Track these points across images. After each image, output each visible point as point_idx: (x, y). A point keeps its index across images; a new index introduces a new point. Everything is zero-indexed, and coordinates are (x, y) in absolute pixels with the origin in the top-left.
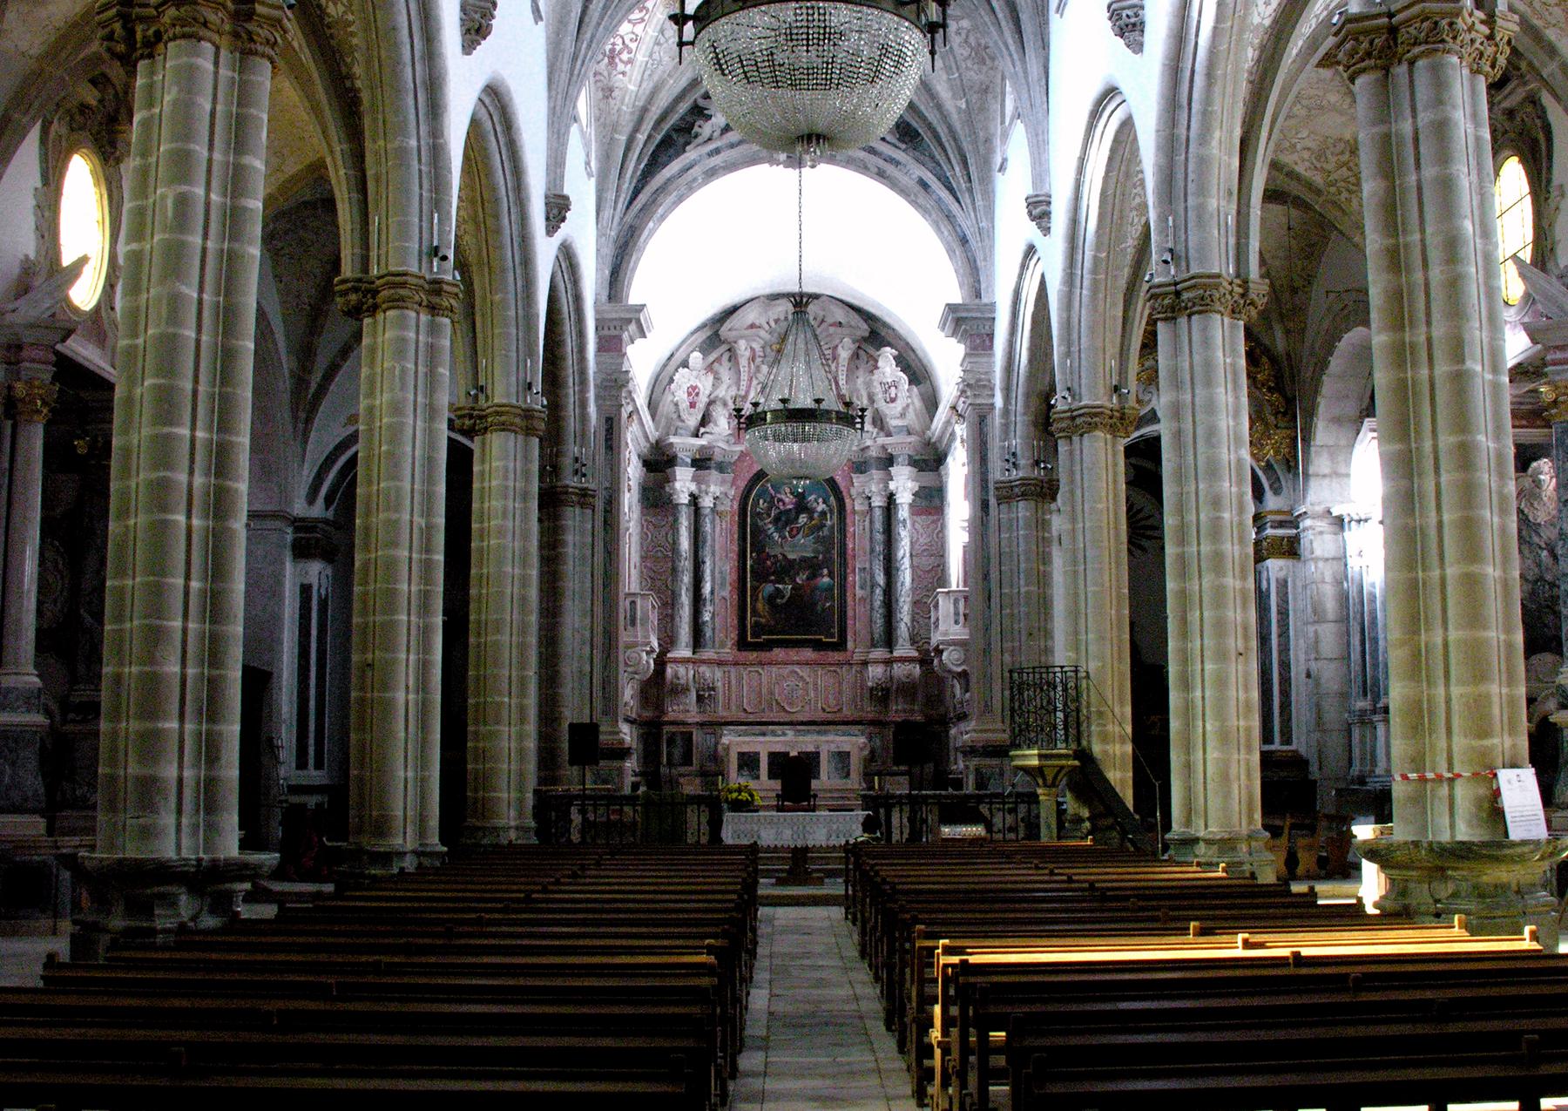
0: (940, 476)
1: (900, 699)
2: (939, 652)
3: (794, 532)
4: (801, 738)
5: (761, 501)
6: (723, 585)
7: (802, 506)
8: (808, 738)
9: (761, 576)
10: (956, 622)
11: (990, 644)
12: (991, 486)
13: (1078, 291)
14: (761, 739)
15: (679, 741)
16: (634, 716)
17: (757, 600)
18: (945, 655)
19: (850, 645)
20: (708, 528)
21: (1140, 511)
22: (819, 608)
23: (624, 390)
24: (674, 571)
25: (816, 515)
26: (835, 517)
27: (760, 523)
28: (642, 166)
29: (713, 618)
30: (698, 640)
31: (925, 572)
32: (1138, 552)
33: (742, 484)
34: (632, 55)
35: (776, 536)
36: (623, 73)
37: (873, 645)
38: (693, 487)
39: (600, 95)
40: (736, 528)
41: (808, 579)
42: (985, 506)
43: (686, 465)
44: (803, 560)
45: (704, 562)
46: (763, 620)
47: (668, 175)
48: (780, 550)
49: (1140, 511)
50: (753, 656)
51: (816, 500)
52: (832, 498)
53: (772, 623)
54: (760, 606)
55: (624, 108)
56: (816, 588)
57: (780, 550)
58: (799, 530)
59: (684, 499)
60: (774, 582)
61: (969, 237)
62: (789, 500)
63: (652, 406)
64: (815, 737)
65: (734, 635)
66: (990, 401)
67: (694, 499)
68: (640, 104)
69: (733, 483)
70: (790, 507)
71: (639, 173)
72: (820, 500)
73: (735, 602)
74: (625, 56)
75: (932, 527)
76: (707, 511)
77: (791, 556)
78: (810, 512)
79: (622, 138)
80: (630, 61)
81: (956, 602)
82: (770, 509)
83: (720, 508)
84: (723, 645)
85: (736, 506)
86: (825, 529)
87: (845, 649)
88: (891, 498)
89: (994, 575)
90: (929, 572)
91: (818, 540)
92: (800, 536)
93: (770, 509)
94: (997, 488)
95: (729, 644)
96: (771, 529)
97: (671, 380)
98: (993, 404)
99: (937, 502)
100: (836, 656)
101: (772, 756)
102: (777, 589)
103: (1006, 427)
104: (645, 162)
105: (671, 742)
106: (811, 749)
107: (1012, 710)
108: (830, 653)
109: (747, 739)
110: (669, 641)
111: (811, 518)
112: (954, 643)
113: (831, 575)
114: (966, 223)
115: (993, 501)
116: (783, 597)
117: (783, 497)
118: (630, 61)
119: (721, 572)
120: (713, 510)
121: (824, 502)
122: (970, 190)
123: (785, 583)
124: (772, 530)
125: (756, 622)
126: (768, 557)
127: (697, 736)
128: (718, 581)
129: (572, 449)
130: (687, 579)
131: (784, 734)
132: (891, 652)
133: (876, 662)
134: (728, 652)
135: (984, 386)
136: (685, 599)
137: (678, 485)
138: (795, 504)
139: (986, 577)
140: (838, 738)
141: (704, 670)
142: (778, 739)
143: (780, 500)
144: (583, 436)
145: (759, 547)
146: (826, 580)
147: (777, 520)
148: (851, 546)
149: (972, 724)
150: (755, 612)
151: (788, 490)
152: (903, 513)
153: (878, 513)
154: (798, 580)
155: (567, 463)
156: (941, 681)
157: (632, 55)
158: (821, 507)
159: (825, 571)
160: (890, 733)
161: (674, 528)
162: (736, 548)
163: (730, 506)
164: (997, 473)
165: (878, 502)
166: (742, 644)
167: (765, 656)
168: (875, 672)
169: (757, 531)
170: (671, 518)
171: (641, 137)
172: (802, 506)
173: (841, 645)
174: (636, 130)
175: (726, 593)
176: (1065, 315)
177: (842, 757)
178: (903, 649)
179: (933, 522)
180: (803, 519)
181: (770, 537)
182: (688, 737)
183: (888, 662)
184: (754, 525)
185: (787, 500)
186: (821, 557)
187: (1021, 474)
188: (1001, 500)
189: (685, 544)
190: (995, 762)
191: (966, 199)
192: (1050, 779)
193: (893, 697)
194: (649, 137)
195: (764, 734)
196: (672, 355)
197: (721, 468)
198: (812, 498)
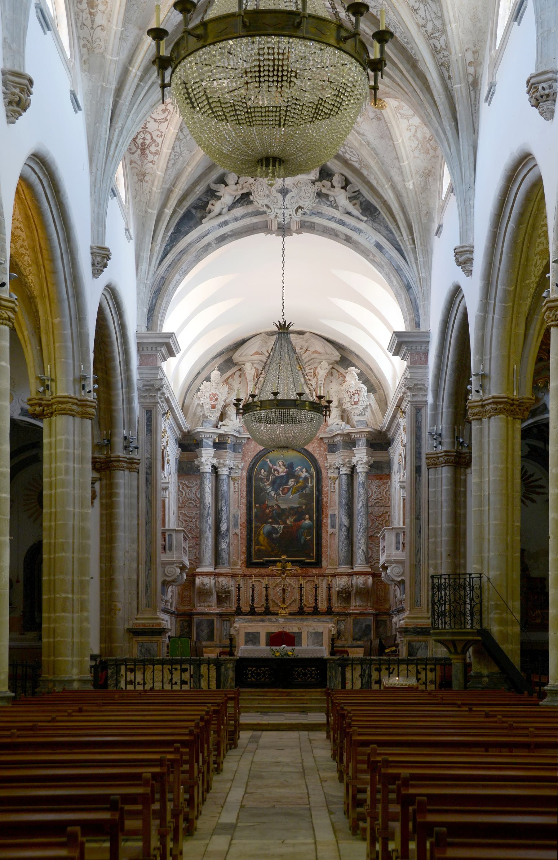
0: (388, 452)
1: (358, 599)
2: (385, 568)
3: (286, 490)
4: (289, 623)
5: (262, 471)
6: (236, 525)
7: (291, 473)
8: (294, 623)
9: (263, 519)
10: (397, 548)
11: (420, 561)
12: (423, 457)
13: (491, 315)
14: (262, 624)
15: (205, 626)
16: (173, 609)
17: (259, 534)
18: (389, 570)
19: (324, 564)
20: (225, 488)
21: (532, 475)
22: (302, 541)
23: (160, 392)
24: (201, 517)
25: (301, 480)
26: (315, 480)
27: (262, 485)
28: (169, 234)
29: (228, 546)
30: (217, 559)
31: (377, 517)
32: (527, 502)
33: (249, 459)
34: (158, 148)
35: (273, 493)
36: (153, 162)
37: (339, 565)
38: (214, 461)
40: (244, 488)
41: (295, 521)
42: (418, 470)
43: (208, 446)
44: (292, 509)
45: (222, 510)
46: (263, 548)
48: (276, 502)
49: (532, 475)
50: (256, 571)
51: (301, 470)
52: (312, 469)
53: (270, 549)
54: (261, 538)
56: (300, 527)
57: (276, 502)
58: (289, 489)
59: (208, 469)
60: (271, 523)
62: (282, 470)
63: (183, 408)
64: (299, 623)
65: (243, 557)
66: (424, 399)
67: (215, 469)
69: (244, 456)
70: (283, 474)
71: (167, 239)
72: (304, 470)
73: (244, 537)
74: (153, 149)
75: (382, 487)
76: (224, 477)
77: (283, 506)
78: (297, 478)
81: (397, 535)
82: (268, 476)
83: (233, 475)
84: (235, 564)
85: (245, 474)
86: (307, 489)
87: (321, 567)
88: (353, 468)
89: (424, 516)
90: (380, 517)
91: (301, 496)
92: (290, 493)
93: (268, 476)
94: (427, 458)
95: (240, 563)
96: (269, 489)
97: (199, 390)
98: (426, 401)
99: (386, 471)
100: (315, 571)
101: (268, 634)
102: (273, 527)
103: (435, 418)
104: (171, 231)
105: (199, 625)
106: (295, 630)
107: (433, 604)
108: (310, 570)
109: (251, 624)
110: (198, 560)
111: (298, 482)
112: (396, 562)
113: (311, 519)
115: (424, 468)
116: (278, 532)
117: (278, 468)
119: (234, 516)
120: (229, 476)
121: (306, 472)
123: (279, 524)
124: (270, 489)
125: (259, 550)
126: (268, 507)
127: (217, 623)
128: (232, 523)
129: (122, 431)
130: (210, 521)
131: (277, 621)
132: (352, 568)
133: (341, 575)
134: (240, 568)
135: (421, 389)
136: (209, 535)
137: (203, 460)
138: (287, 472)
139: (418, 518)
140: (315, 624)
141: (223, 580)
142: (273, 624)
143: (275, 470)
144: (130, 424)
145: (261, 500)
146: (307, 522)
147: (273, 483)
148: (325, 500)
149: (407, 614)
150: (258, 543)
151: (281, 463)
152: (361, 478)
153: (344, 478)
154: (288, 522)
155: (119, 442)
156: (386, 587)
157: (158, 148)
158: (304, 474)
159: (307, 516)
160: (350, 621)
161: (201, 488)
162: (244, 501)
163: (241, 474)
164: (428, 446)
165: (344, 471)
166: (249, 563)
167: (263, 571)
168: (341, 583)
169: (260, 490)
170: (198, 481)
171: (168, 212)
172: (291, 473)
173: (318, 564)
174: (164, 205)
175: (238, 531)
176: (480, 334)
177: (318, 635)
178: (360, 566)
179: (383, 484)
180: (291, 482)
181: (268, 494)
182: (211, 623)
183: (350, 575)
184: (258, 487)
185: (280, 470)
186: (304, 507)
187: (444, 449)
188: (429, 466)
189: (209, 499)
190: (421, 638)
192: (459, 649)
193: (353, 598)
194: (174, 212)
195: (263, 621)
196: (199, 373)
197: (235, 448)
198: (298, 468)
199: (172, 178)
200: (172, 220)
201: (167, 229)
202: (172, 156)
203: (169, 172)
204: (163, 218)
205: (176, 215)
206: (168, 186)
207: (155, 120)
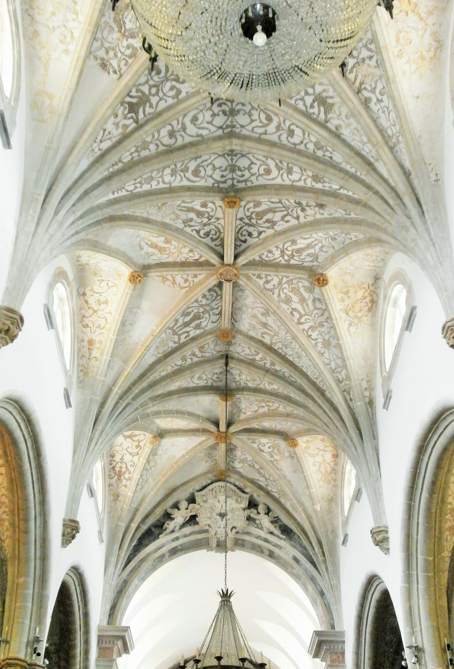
28: (134, 544)
34: (131, 475)
36: (126, 486)
39: (112, 498)
47: (148, 552)
55: (125, 506)
61: (325, 591)
68: (134, 506)
71: (131, 548)
74: (127, 476)
79: (123, 525)
80: (130, 479)
114: (324, 585)
118: (130, 479)
122: (325, 561)
157: (131, 475)
171: (134, 526)
174: (131, 520)
191: (322, 567)
199: (139, 499)
200: (137, 533)
201: (131, 540)
202: (140, 482)
203: (137, 494)
204: (129, 530)
205: (140, 529)
206: (135, 506)
207: (130, 453)
